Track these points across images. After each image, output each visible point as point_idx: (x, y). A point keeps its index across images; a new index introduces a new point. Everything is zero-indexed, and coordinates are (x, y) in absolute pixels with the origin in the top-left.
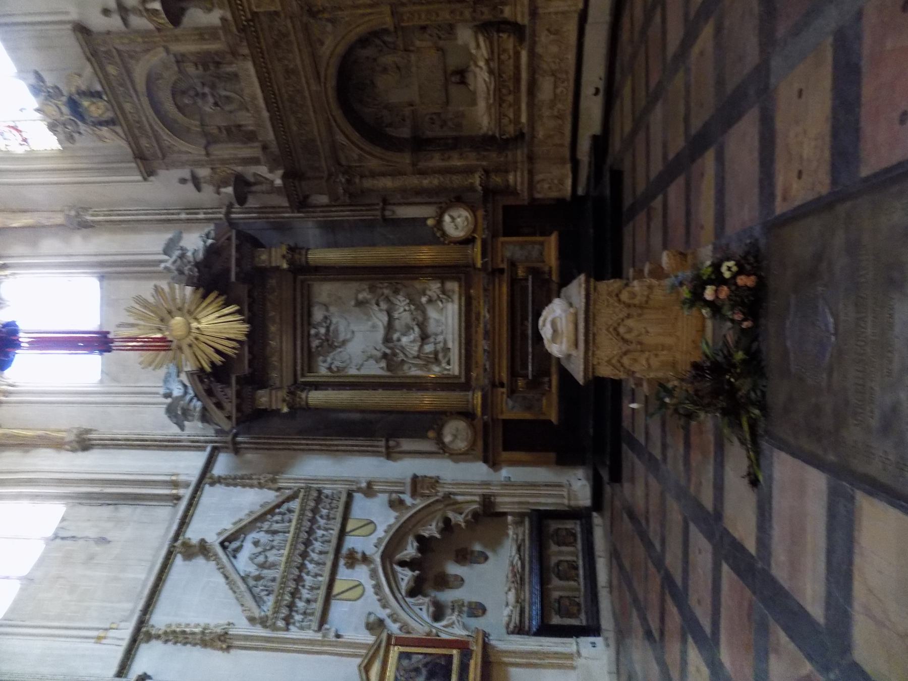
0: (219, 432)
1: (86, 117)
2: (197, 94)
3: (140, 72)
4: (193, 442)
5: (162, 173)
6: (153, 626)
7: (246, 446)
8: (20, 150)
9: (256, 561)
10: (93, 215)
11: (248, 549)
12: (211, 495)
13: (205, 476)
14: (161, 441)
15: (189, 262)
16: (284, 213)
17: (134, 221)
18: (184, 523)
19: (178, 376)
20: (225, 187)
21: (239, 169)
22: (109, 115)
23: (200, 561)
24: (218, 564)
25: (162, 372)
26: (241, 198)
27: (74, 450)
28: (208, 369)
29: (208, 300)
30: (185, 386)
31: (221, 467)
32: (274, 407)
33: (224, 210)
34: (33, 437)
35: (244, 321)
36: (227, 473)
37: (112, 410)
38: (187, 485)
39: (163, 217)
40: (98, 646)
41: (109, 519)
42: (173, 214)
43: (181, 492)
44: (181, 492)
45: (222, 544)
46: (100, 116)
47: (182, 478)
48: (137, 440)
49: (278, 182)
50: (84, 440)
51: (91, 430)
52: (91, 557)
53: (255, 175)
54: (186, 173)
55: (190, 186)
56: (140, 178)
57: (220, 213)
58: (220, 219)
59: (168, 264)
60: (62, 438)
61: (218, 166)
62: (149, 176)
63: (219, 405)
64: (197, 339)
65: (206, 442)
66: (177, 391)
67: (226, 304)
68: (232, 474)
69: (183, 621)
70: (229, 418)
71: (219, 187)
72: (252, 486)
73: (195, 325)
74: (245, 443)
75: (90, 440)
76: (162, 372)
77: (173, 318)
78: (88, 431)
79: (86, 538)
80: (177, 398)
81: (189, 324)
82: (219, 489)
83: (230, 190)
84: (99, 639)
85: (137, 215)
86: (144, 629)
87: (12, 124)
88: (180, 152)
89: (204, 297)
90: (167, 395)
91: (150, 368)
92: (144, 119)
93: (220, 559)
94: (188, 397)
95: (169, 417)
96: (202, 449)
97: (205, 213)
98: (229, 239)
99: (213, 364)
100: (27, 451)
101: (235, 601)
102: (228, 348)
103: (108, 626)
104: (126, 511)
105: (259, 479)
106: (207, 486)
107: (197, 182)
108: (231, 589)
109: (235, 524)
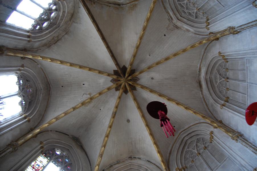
100: (16, 47)
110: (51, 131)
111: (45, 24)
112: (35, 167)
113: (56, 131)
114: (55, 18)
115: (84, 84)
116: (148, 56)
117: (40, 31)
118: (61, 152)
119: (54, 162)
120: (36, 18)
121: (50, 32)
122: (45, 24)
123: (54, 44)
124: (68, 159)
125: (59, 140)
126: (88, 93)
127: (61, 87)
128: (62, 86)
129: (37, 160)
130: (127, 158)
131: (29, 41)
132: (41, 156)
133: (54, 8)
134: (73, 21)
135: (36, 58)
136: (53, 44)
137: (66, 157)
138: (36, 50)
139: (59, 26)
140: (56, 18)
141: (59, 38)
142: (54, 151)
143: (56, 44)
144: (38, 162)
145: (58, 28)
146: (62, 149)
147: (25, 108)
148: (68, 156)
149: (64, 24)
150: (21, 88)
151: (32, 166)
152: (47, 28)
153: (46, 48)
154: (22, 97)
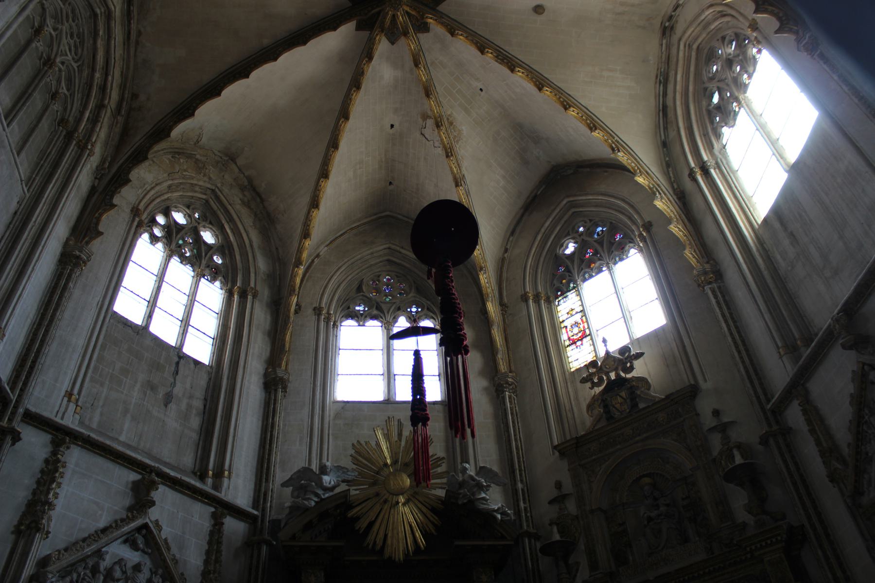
0: (276, 525)
4: (265, 494)
6: (68, 448)
8: (564, 337)
9: (117, 568)
10: (510, 397)
11: (132, 557)
12: (200, 515)
13: (224, 508)
15: (473, 494)
17: (509, 436)
18: (176, 484)
19: (343, 481)
20: (559, 532)
21: (582, 547)
23: (128, 502)
24: (122, 520)
25: (347, 463)
26: (547, 549)
27: (266, 375)
28: (350, 514)
30: (332, 489)
31: (233, 527)
33: (532, 530)
34: (284, 340)
35: (407, 555)
37: (306, 411)
38: (217, 487)
40: (63, 393)
41: (189, 406)
42: (521, 475)
43: (210, 481)
44: (210, 481)
45: (145, 526)
47: (226, 481)
48: (271, 435)
52: (153, 388)
54: (568, 486)
55: (555, 493)
57: (528, 526)
58: (521, 526)
60: (280, 366)
63: (308, 526)
64: (385, 501)
65: (264, 510)
67: (425, 534)
69: (65, 481)
70: (293, 537)
71: (557, 525)
72: (206, 562)
73: (402, 499)
75: (276, 390)
76: (347, 463)
77: (409, 476)
79: (174, 384)
81: (402, 494)
82: (206, 524)
83: (557, 537)
84: (69, 394)
85: (516, 440)
86: (68, 439)
87: (588, 332)
89: (433, 510)
90: (323, 470)
92: (619, 447)
93: (127, 524)
94: (320, 492)
96: (255, 505)
97: (525, 509)
99: (357, 519)
101: (73, 540)
103: (79, 404)
104: (195, 422)
106: (213, 510)
107: (559, 500)
108: (89, 536)
109: (166, 540)
110: (506, 250)
111: (208, 237)
112: (575, 337)
113: (513, 233)
114: (188, 207)
115: (392, 126)
119: (587, 276)
120: (192, 274)
121: (231, 220)
122: (208, 237)
123: (262, 201)
124: (598, 226)
125: (538, 234)
126: (420, 120)
127: (391, 187)
128: (391, 183)
129: (563, 321)
130: (664, 41)
133: (161, 219)
134: (195, 144)
135: (305, 255)
137: (590, 232)
138: (277, 264)
139: (213, 190)
140: (188, 208)
141: (246, 183)
142: (559, 260)
143: (263, 196)
144: (568, 323)
145: (219, 193)
146: (569, 232)
147: (428, 309)
148: (591, 221)
149: (205, 175)
150: (375, 312)
151: (570, 345)
154: (399, 312)
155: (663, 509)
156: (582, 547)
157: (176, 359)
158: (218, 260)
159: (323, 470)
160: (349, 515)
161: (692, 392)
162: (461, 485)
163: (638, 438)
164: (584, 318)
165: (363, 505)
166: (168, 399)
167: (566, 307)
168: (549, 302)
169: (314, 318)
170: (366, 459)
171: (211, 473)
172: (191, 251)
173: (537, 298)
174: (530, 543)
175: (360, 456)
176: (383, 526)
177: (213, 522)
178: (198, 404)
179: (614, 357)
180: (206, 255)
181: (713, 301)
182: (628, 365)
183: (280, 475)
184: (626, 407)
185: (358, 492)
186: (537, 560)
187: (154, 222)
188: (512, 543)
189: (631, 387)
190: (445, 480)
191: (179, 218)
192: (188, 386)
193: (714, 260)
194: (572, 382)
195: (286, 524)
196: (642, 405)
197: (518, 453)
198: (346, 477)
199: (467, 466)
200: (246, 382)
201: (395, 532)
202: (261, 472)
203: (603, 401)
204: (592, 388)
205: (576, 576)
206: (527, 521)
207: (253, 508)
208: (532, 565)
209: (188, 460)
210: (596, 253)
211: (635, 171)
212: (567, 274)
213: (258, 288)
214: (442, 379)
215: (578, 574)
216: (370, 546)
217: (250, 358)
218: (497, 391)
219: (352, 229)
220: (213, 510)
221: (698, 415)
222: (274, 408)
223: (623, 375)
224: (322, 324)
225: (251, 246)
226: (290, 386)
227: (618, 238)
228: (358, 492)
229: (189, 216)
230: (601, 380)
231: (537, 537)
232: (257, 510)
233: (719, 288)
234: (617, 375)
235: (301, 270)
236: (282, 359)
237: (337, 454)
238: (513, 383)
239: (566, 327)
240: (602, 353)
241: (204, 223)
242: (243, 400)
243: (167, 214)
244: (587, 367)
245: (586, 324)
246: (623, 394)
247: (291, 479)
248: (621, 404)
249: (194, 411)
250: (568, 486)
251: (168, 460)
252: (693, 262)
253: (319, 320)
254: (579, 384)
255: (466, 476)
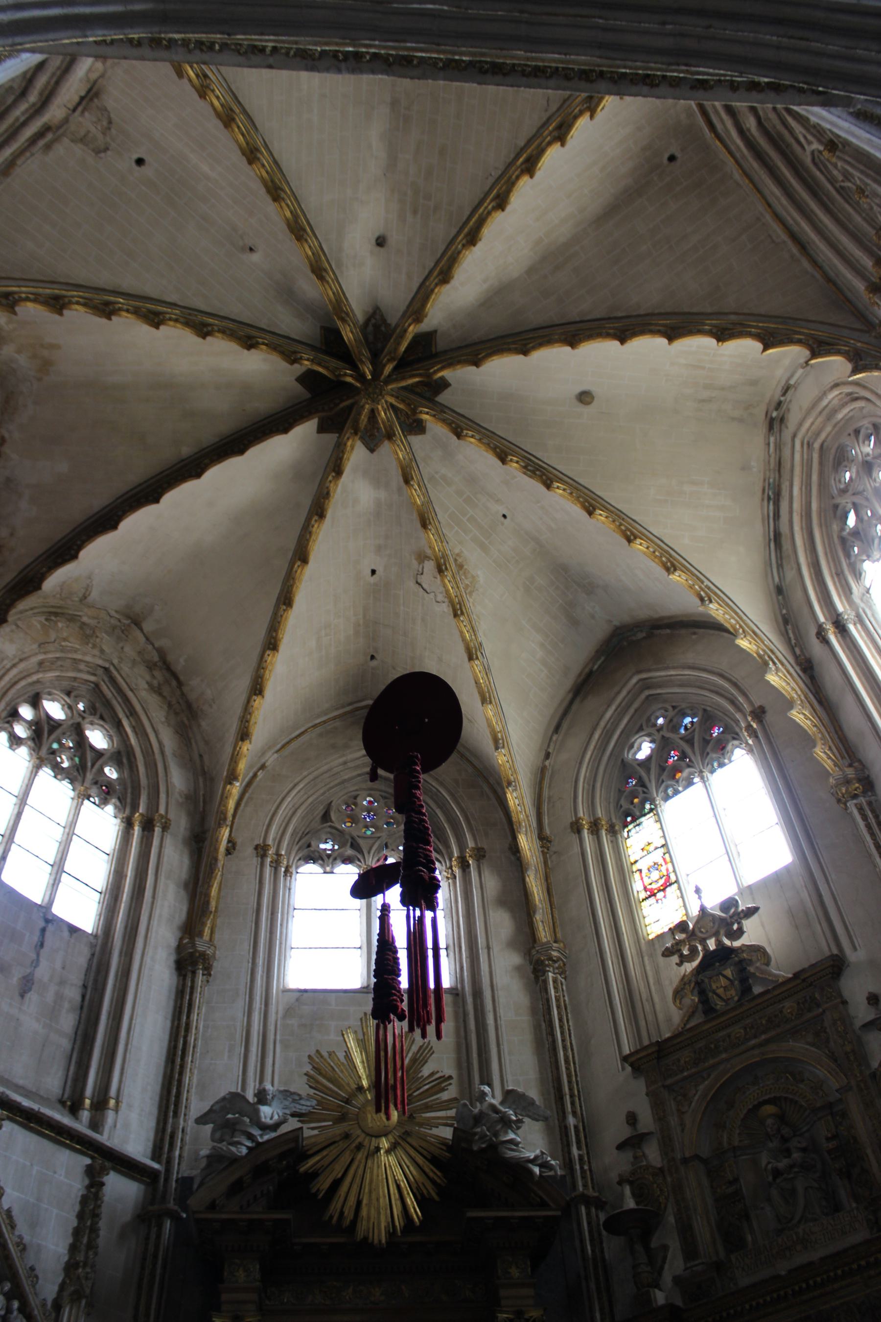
1: (707, 973)
2: (784, 1140)
3: (799, 1048)
4: (172, 1136)
5: (640, 1086)
7: (153, 1236)
8: (637, 886)
12: (67, 1169)
14: (180, 1082)
16: (602, 1310)
17: (554, 1041)
19: (293, 1115)
20: (634, 1195)
21: (671, 1219)
22: (720, 1005)
25: (300, 1086)
26: (616, 1224)
27: (179, 948)
29: (428, 1167)
30: (275, 1127)
31: (120, 1189)
32: (224, 1297)
33: (591, 1192)
34: (207, 895)
35: (391, 1234)
36: (106, 1199)
37: (241, 1004)
38: (96, 1125)
39: (566, 1089)
41: (59, 997)
42: (573, 1103)
43: (85, 1115)
44: (85, 1115)
46: (714, 992)
47: (110, 1115)
48: (185, 1043)
49: (660, 1298)
50: (194, 963)
51: (210, 975)
53: (665, 1248)
54: (647, 1121)
55: (626, 1132)
56: (626, 1051)
57: (585, 1186)
58: (574, 1186)
59: (489, 1099)
60: (201, 934)
61: (669, 1179)
62: (631, 1065)
63: (236, 1188)
64: (359, 1147)
66: (267, 1113)
67: (421, 1201)
68: (104, 1210)
70: (212, 1206)
71: (631, 1183)
72: (73, 1248)
73: (385, 1143)
74: (159, 1236)
75: (194, 973)
76: (300, 1086)
78: (208, 970)
79: (36, 963)
80: (257, 1112)
81: (385, 1135)
82: (77, 1185)
83: (630, 1204)
85: (565, 1048)
87: (673, 878)
88: (681, 1113)
89: (434, 1160)
90: (262, 1097)
91: (308, 1068)
92: (724, 1056)
94: (256, 1132)
95: (224, 1099)
96: (156, 1154)
97: (581, 1158)
98: (543, 1205)
99: (313, 1175)
100: (186, 885)
102: (343, 1203)
104: (68, 1022)
105: (85, 1265)
106: (88, 1161)
107: (632, 1143)
110: (547, 756)
111: (97, 738)
112: (654, 886)
114: (68, 694)
115: (373, 572)
116: (255, 257)
117: (125, 761)
118: (648, 735)
120: (72, 794)
121: (132, 713)
122: (97, 738)
123: (180, 684)
124: (685, 715)
125: (594, 729)
126: (415, 563)
127: (374, 663)
128: (373, 657)
129: (636, 862)
130: (772, 439)
131: (165, 828)
132: (628, 837)
133: (26, 712)
134: (81, 601)
135: (242, 766)
136: (183, 694)
137: (673, 725)
138: (201, 780)
139: (106, 669)
140: (69, 693)
141: (156, 658)
143: (182, 678)
144: (643, 865)
146: (641, 725)
148: (674, 707)
149: (94, 646)
150: (349, 852)
151: (647, 898)
152: (115, 726)
153: (199, 726)
155: (796, 1155)
156: (671, 1219)
157: (42, 924)
158: (111, 773)
159: (262, 1097)
160: (302, 1170)
161: (835, 967)
162: (478, 1119)
163: (753, 1042)
164: (667, 856)
165: (325, 1153)
166: (26, 985)
167: (640, 839)
168: (613, 831)
169: (256, 861)
170: (329, 1080)
171: (87, 1102)
172: (71, 759)
173: (595, 828)
174: (588, 1214)
175: (320, 1074)
176: (355, 1187)
177: (87, 1182)
178: (73, 994)
179: (713, 915)
180: (93, 765)
181: (861, 824)
182: (735, 927)
183: (196, 1104)
184: (733, 992)
185: (316, 1132)
186: (601, 1243)
187: (14, 715)
188: (559, 1213)
189: (741, 961)
190: (452, 1113)
191: (55, 710)
192: (58, 965)
193: (860, 761)
194: (651, 956)
195: (201, 1184)
196: (757, 990)
197: (568, 1069)
198: (298, 1108)
199: (487, 1089)
200: (148, 960)
201: (374, 1196)
202: (168, 1100)
203: (698, 983)
204: (680, 964)
205: (662, 1268)
206: (584, 1177)
207: (153, 1159)
208: (593, 1251)
209: (53, 1082)
210: (683, 756)
211: (736, 630)
212: (640, 789)
213: (171, 816)
214: (452, 954)
215: (666, 1266)
216: (335, 1219)
217: (155, 922)
218: (535, 971)
219: (315, 726)
220: (88, 1161)
221: (845, 1002)
222: (191, 1000)
223: (727, 942)
224: (268, 870)
225: (162, 753)
226: (217, 967)
227: (716, 732)
228: (316, 1132)
229: (70, 707)
230: (693, 951)
231: (600, 1204)
232: (159, 1162)
233: (870, 804)
234: (719, 943)
235: (236, 789)
236: (204, 924)
237: (285, 1072)
238: (559, 959)
239: (640, 871)
240: (695, 911)
241: (91, 718)
242: (143, 988)
243: (35, 702)
244: (672, 931)
245: (670, 866)
246: (728, 972)
247: (211, 1111)
248: (725, 988)
249: (66, 1005)
250: (647, 1121)
251: (21, 1082)
252: (828, 765)
253: (262, 865)
254: (661, 959)
255: (485, 1105)
